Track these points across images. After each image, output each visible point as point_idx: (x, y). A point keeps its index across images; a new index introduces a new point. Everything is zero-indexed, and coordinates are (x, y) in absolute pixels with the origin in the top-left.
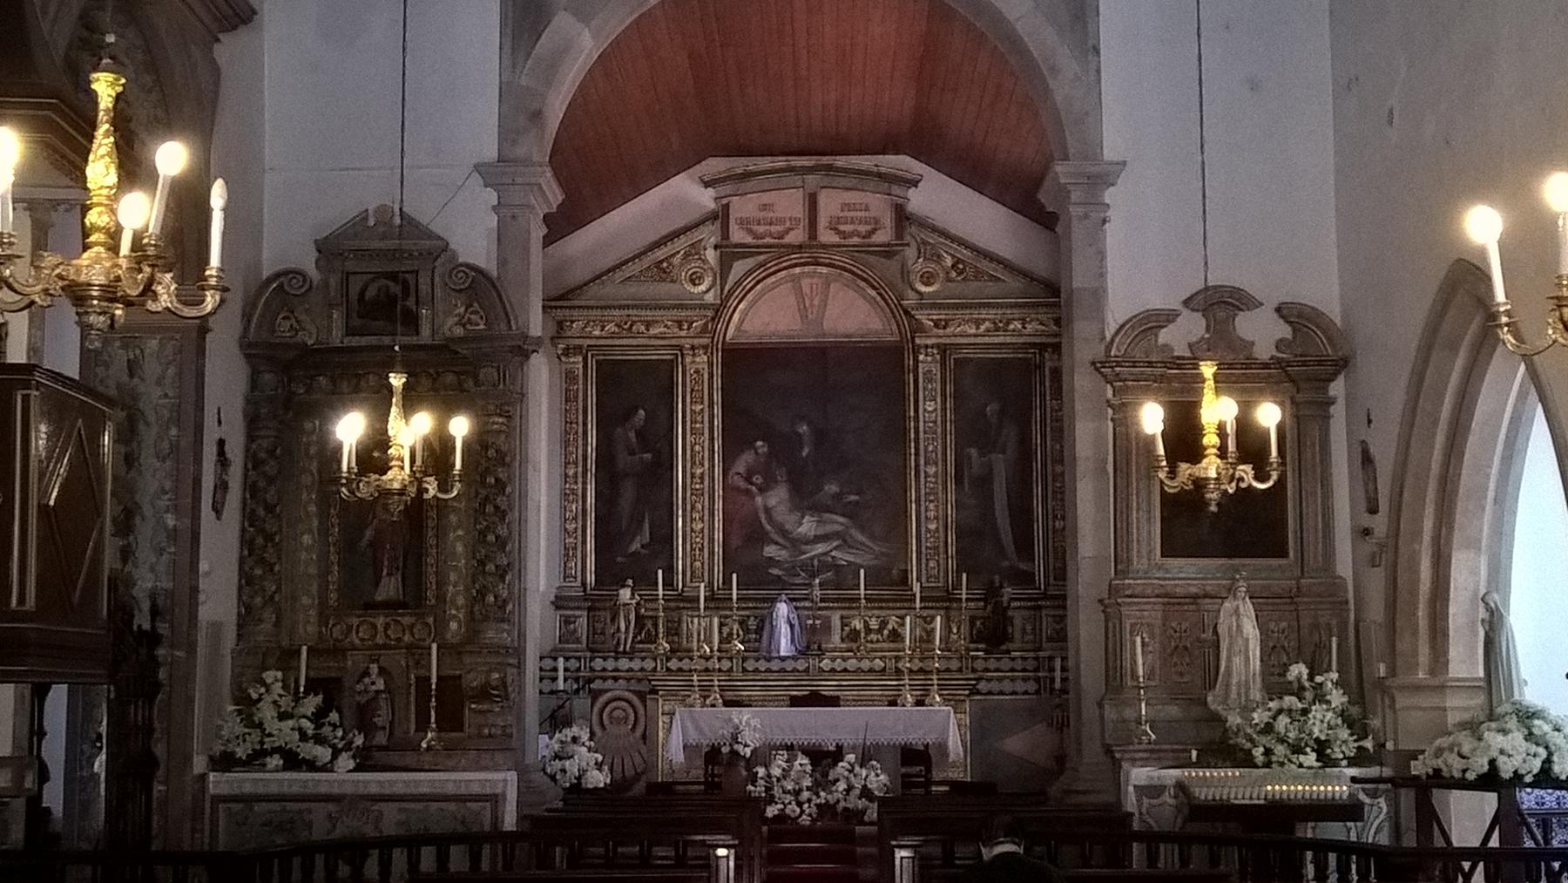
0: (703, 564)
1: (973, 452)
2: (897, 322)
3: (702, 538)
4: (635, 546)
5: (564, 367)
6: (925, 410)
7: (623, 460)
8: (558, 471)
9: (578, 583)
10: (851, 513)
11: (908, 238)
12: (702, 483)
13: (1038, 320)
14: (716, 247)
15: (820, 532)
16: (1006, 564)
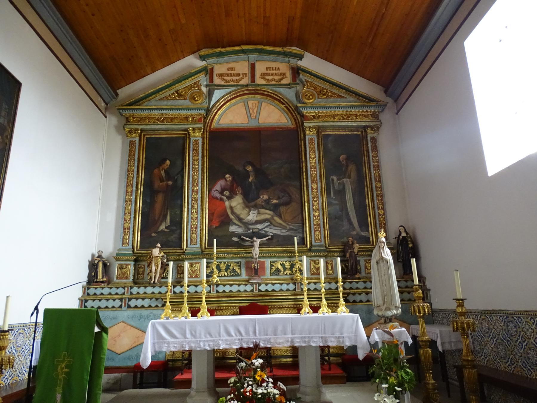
0: (197, 236)
1: (335, 178)
2: (295, 119)
4: (162, 227)
5: (129, 139)
6: (310, 157)
7: (157, 184)
8: (123, 190)
9: (130, 246)
10: (275, 208)
11: (298, 82)
12: (197, 194)
13: (363, 115)
15: (259, 218)
16: (354, 233)
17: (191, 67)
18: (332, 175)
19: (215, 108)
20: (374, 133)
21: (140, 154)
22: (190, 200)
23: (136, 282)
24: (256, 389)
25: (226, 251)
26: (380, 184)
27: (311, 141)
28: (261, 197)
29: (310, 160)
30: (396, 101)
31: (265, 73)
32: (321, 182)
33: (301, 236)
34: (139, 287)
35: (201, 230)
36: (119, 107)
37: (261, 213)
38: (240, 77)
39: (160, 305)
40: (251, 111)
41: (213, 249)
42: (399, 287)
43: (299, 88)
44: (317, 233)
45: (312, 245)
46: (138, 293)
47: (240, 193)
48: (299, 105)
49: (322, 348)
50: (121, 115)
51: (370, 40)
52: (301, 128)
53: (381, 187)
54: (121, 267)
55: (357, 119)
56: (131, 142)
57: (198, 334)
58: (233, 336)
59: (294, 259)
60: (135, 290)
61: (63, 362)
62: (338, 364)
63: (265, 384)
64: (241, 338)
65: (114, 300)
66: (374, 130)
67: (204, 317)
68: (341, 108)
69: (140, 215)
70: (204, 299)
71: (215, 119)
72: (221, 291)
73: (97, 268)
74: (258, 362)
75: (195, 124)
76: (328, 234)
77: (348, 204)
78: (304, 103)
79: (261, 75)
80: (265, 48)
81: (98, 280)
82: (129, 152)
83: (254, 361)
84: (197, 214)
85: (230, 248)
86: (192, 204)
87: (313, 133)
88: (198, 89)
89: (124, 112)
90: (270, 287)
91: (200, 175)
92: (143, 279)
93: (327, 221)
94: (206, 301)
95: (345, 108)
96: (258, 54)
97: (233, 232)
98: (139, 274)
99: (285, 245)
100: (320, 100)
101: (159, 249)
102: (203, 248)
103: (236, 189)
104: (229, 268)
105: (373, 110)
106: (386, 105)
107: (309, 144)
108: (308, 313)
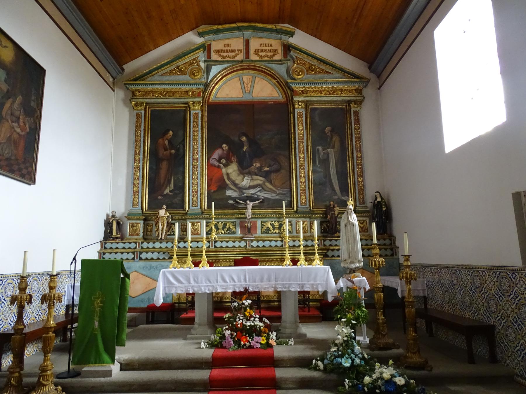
0: (197, 199)
1: (320, 148)
2: (285, 93)
3: (197, 187)
4: (167, 191)
6: (298, 129)
7: (162, 153)
8: (132, 158)
9: (140, 208)
10: (266, 175)
11: (289, 58)
12: (198, 162)
13: (347, 90)
14: (205, 62)
16: (336, 197)
17: (190, 43)
18: (318, 146)
19: (212, 83)
20: (357, 107)
21: (146, 124)
22: (191, 167)
23: (146, 238)
24: (246, 323)
25: (223, 212)
26: (361, 154)
27: (300, 114)
28: (254, 165)
29: (298, 132)
30: (379, 76)
31: (259, 50)
32: (308, 151)
33: (289, 200)
34: (148, 243)
35: (201, 194)
36: (126, 83)
37: (253, 179)
38: (236, 53)
39: (167, 258)
40: (246, 86)
41: (212, 210)
42: (362, 245)
43: (289, 63)
44: (303, 197)
45: (298, 208)
46: (148, 248)
47: (235, 161)
48: (289, 81)
49: (299, 292)
50: (128, 89)
51: (355, 21)
52: (291, 102)
53: (361, 157)
54: (132, 226)
55: (342, 94)
56: (137, 114)
57: (200, 281)
58: (228, 283)
59: (282, 220)
60: (145, 245)
61: (99, 298)
62: (317, 308)
63: (252, 319)
64: (234, 284)
65: (128, 253)
66: (357, 105)
67: (205, 267)
68: (327, 84)
69: (147, 180)
70: (204, 253)
71: (213, 93)
72: (218, 246)
73: (112, 226)
74: (248, 302)
75: (194, 98)
76: (313, 198)
77: (331, 172)
78: (294, 79)
79: (255, 52)
80: (259, 25)
81: (113, 236)
82: (136, 124)
83: (244, 302)
84: (198, 180)
85: (226, 210)
86: (193, 171)
87: (302, 107)
88: (197, 65)
89: (130, 86)
90: (261, 244)
91: (200, 144)
92: (151, 235)
93: (312, 187)
94: (206, 255)
95: (331, 84)
96: (252, 30)
97: (229, 196)
98: (147, 231)
99: (274, 208)
100: (309, 75)
101: (164, 210)
102: (203, 210)
103: (231, 158)
104: (226, 227)
105: (357, 85)
106: (368, 82)
107: (298, 117)
108: (289, 265)
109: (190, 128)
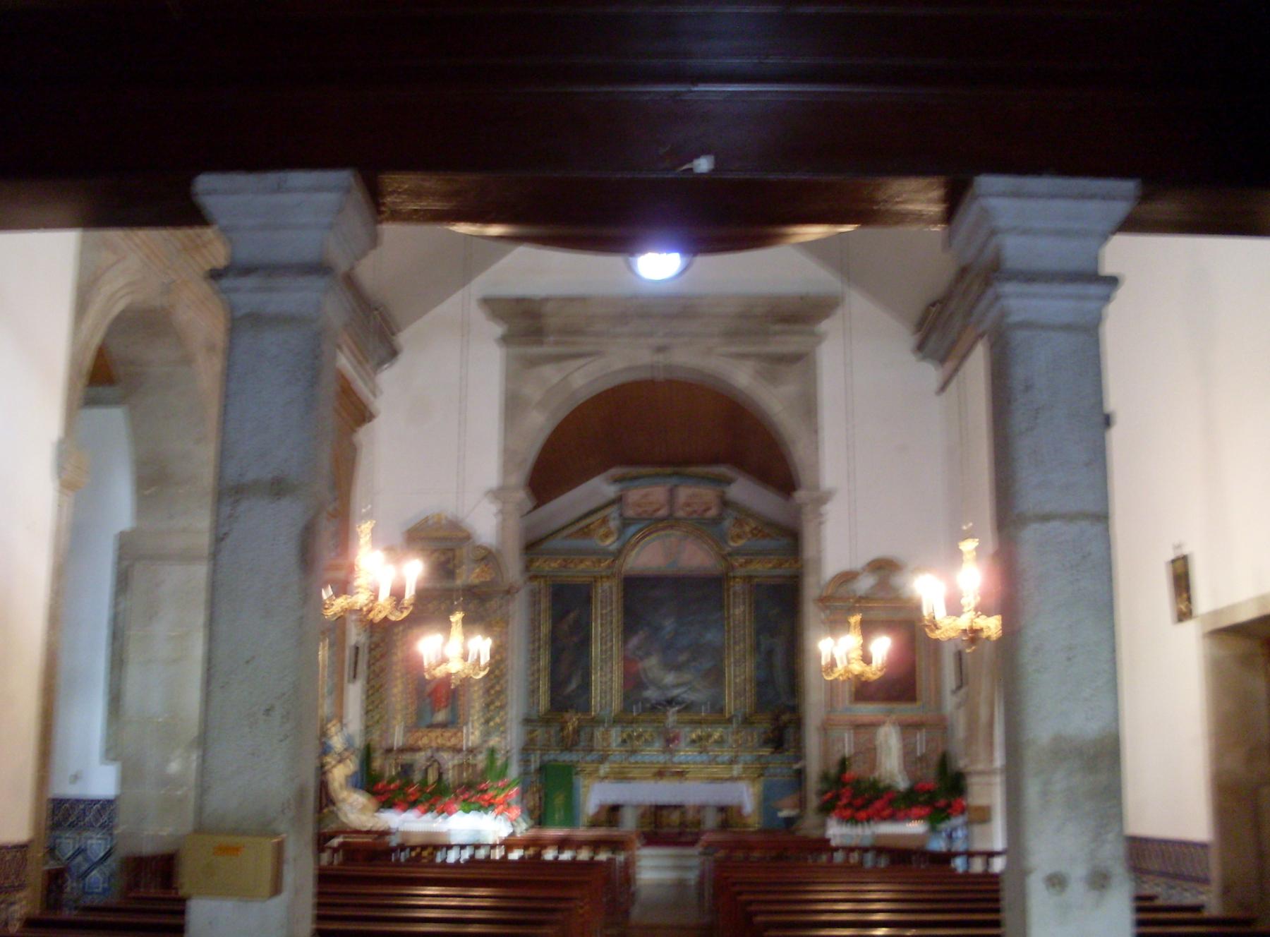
109: (597, 610)
